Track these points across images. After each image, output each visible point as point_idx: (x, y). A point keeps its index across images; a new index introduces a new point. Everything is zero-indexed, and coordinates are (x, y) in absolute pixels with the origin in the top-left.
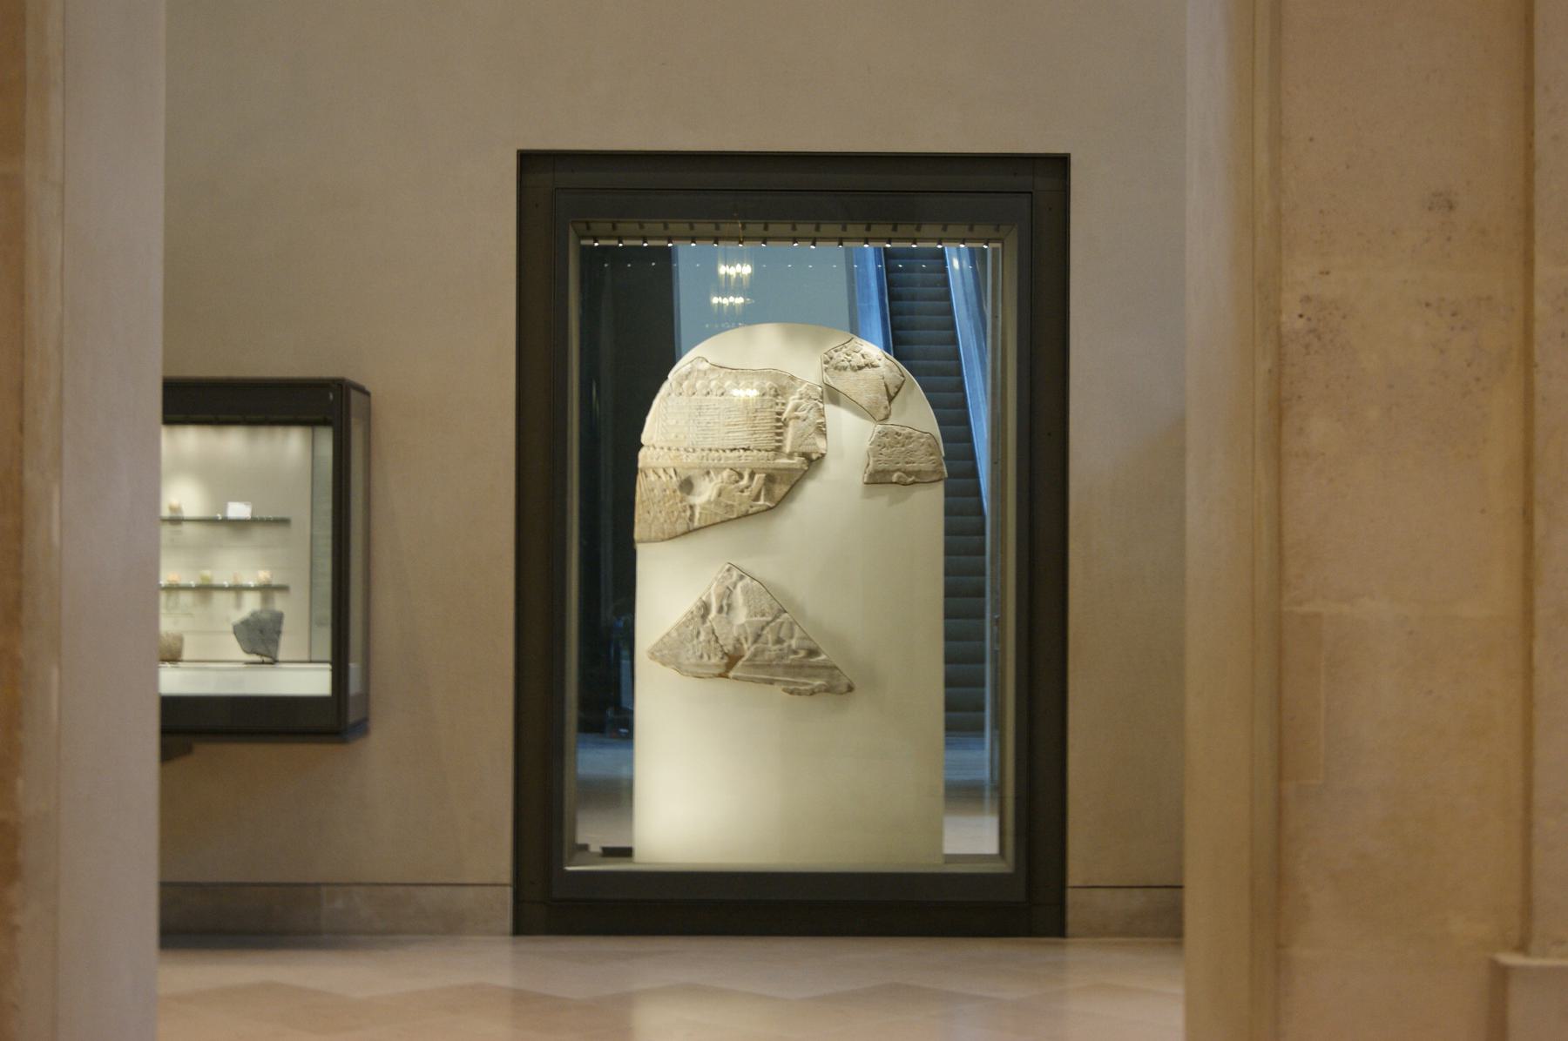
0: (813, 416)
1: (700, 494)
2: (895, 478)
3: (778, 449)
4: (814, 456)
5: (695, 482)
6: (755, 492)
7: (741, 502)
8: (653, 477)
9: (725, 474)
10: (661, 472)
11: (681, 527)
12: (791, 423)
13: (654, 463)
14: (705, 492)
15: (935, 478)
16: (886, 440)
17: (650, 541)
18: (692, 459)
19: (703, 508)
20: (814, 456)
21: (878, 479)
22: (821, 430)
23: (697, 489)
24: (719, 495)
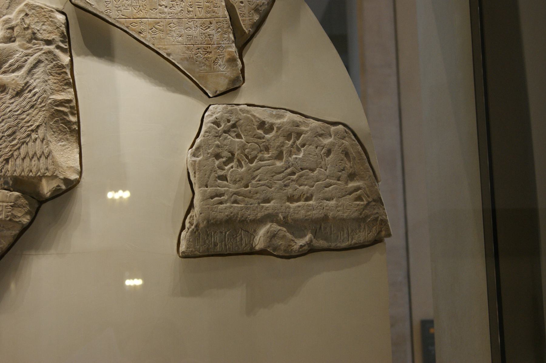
0: (40, 81)
2: (260, 239)
4: (46, 188)
15: (362, 236)
16: (233, 141)
20: (46, 188)
21: (217, 241)
22: (66, 120)
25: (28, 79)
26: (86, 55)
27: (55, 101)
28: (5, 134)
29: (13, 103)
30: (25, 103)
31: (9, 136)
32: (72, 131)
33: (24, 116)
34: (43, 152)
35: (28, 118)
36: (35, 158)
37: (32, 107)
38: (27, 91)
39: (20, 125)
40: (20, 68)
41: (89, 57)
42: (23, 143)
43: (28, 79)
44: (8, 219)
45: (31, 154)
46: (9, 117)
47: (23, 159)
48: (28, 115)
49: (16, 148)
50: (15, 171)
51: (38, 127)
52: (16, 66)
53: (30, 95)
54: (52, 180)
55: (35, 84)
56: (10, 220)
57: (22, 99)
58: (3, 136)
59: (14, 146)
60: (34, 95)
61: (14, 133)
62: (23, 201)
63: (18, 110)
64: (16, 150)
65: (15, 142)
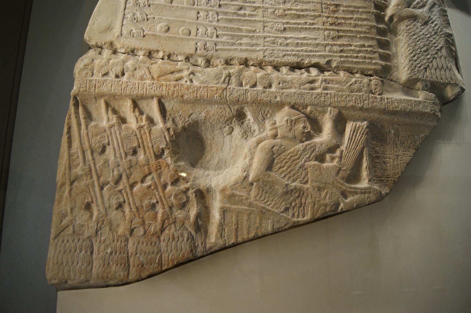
1: (219, 167)
3: (385, 73)
4: (450, 93)
5: (207, 136)
6: (349, 161)
7: (318, 181)
8: (104, 119)
9: (281, 117)
10: (126, 108)
11: (171, 250)
12: (402, 27)
13: (110, 85)
14: (234, 162)
17: (85, 285)
18: (205, 79)
19: (230, 198)
23: (213, 155)
24: (269, 167)
25: (430, 14)
26: (453, 8)
27: (446, 33)
28: (422, 50)
29: (423, 29)
30: (430, 30)
31: (425, 51)
32: (453, 57)
33: (432, 39)
34: (447, 67)
35: (434, 41)
36: (443, 70)
37: (435, 33)
38: (430, 23)
39: (430, 45)
40: (423, 6)
41: (455, 9)
42: (434, 58)
43: (430, 14)
44: (432, 112)
45: (440, 66)
46: (423, 39)
47: (436, 69)
48: (434, 39)
49: (430, 61)
50: (432, 77)
51: (441, 47)
52: (421, 4)
53: (433, 26)
54: (455, 87)
55: (434, 19)
56: (434, 113)
57: (428, 27)
58: (421, 51)
59: (429, 59)
60: (436, 26)
61: (427, 50)
62: (437, 101)
63: (427, 35)
64: (430, 62)
65: (428, 57)
